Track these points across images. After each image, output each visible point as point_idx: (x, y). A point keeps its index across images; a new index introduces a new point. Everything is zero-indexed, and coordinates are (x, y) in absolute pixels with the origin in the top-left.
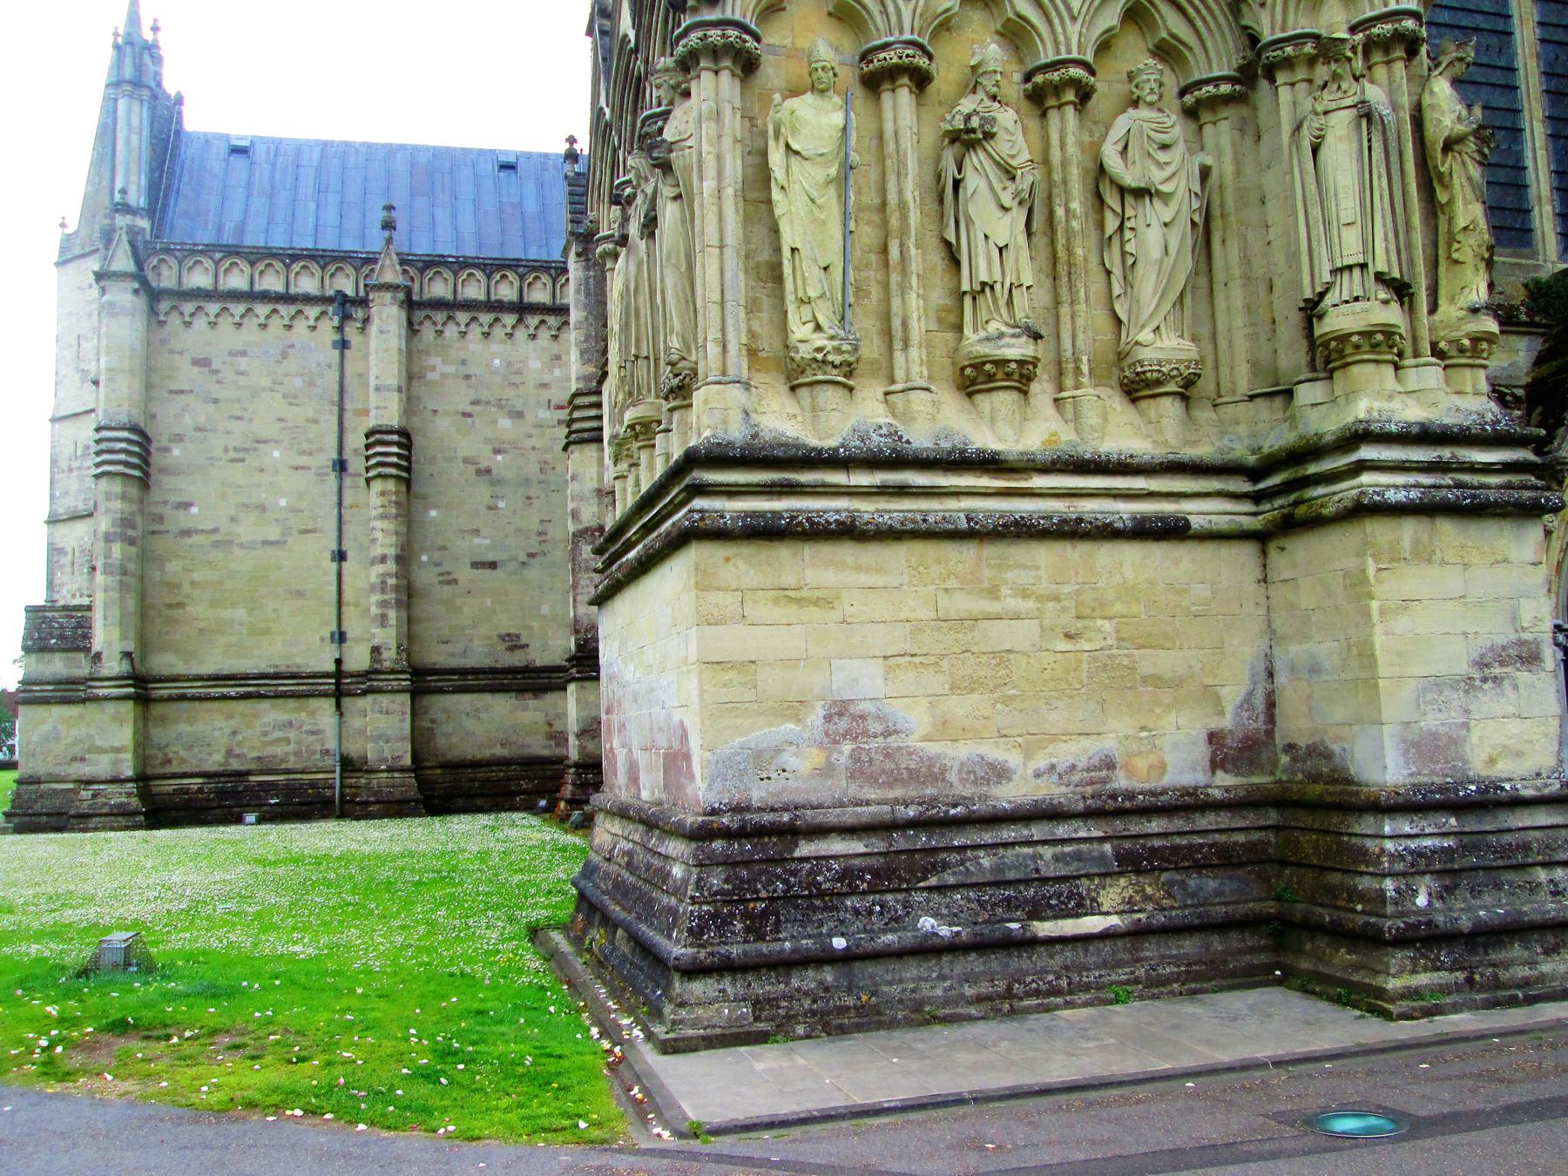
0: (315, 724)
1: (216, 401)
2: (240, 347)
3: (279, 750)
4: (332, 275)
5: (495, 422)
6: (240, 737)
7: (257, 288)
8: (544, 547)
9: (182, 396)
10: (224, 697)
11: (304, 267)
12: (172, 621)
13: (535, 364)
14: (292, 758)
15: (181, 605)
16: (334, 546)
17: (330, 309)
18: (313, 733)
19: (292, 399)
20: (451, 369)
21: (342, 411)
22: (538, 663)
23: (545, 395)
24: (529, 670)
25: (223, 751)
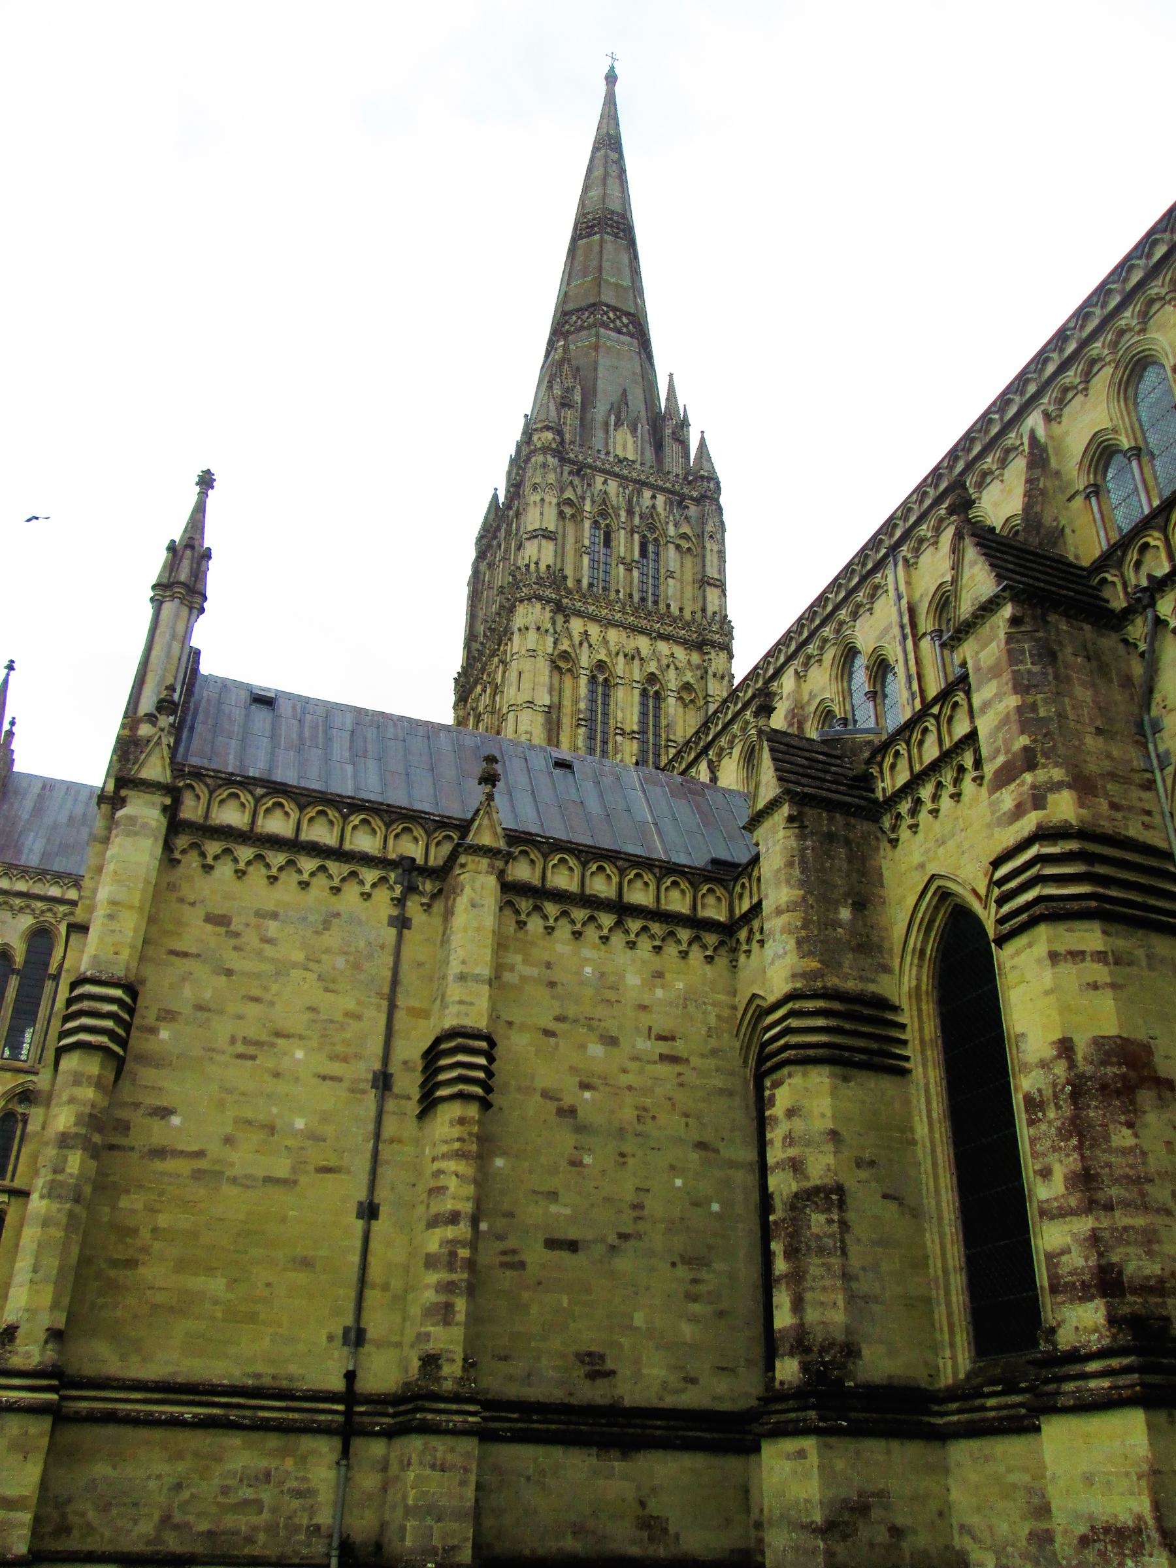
0: (305, 1479)
1: (229, 973)
2: (270, 907)
3: (242, 1522)
4: (397, 836)
5: (583, 1047)
6: (186, 1495)
7: (304, 837)
8: (641, 1226)
9: (185, 961)
10: (175, 1423)
11: (364, 821)
12: (114, 1287)
13: (633, 980)
14: (262, 1537)
15: (132, 1263)
16: (362, 1195)
17: (392, 876)
18: (298, 1494)
19: (328, 983)
20: (534, 972)
21: (392, 1007)
22: (627, 1403)
23: (646, 1019)
24: (615, 1412)
25: (156, 1517)
